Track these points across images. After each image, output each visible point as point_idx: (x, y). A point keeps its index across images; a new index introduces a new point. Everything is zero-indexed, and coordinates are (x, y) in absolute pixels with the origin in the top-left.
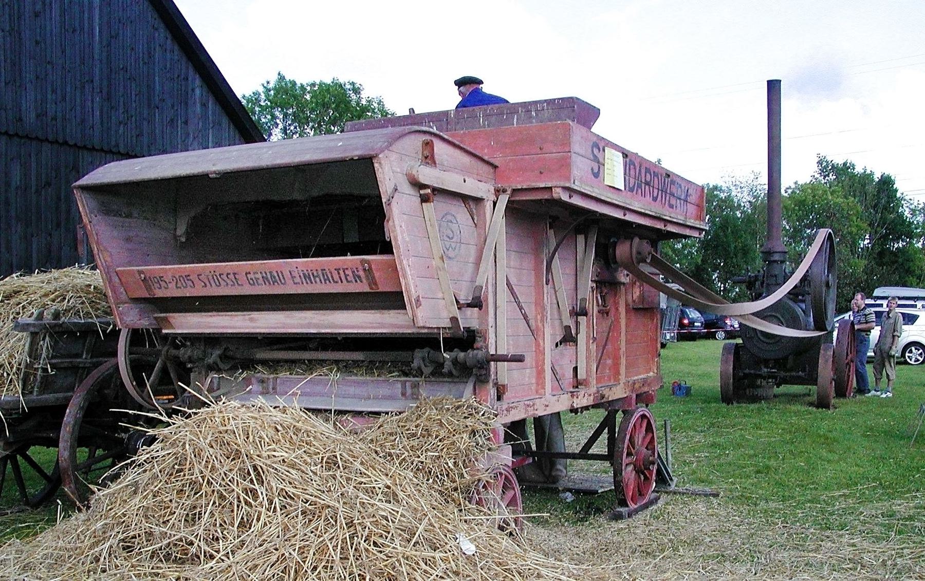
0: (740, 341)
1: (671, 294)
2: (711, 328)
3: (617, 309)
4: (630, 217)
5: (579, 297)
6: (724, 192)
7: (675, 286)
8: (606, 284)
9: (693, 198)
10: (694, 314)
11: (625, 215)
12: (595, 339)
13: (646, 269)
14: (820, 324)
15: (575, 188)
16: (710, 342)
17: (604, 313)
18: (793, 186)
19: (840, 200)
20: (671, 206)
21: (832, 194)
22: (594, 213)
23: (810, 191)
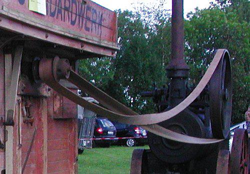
0: (147, 148)
1: (87, 106)
2: (123, 136)
3: (40, 120)
4: (51, 39)
5: (7, 109)
6: (133, 16)
7: (90, 100)
8: (30, 98)
9: (107, 22)
10: (107, 124)
11: (47, 37)
12: (20, 146)
13: (66, 84)
14: (218, 132)
15: (4, 13)
16: (121, 150)
17: (28, 123)
18: (194, 12)
19: (235, 24)
20: (87, 29)
21: (228, 19)
22: (20, 35)
23: (208, 16)
